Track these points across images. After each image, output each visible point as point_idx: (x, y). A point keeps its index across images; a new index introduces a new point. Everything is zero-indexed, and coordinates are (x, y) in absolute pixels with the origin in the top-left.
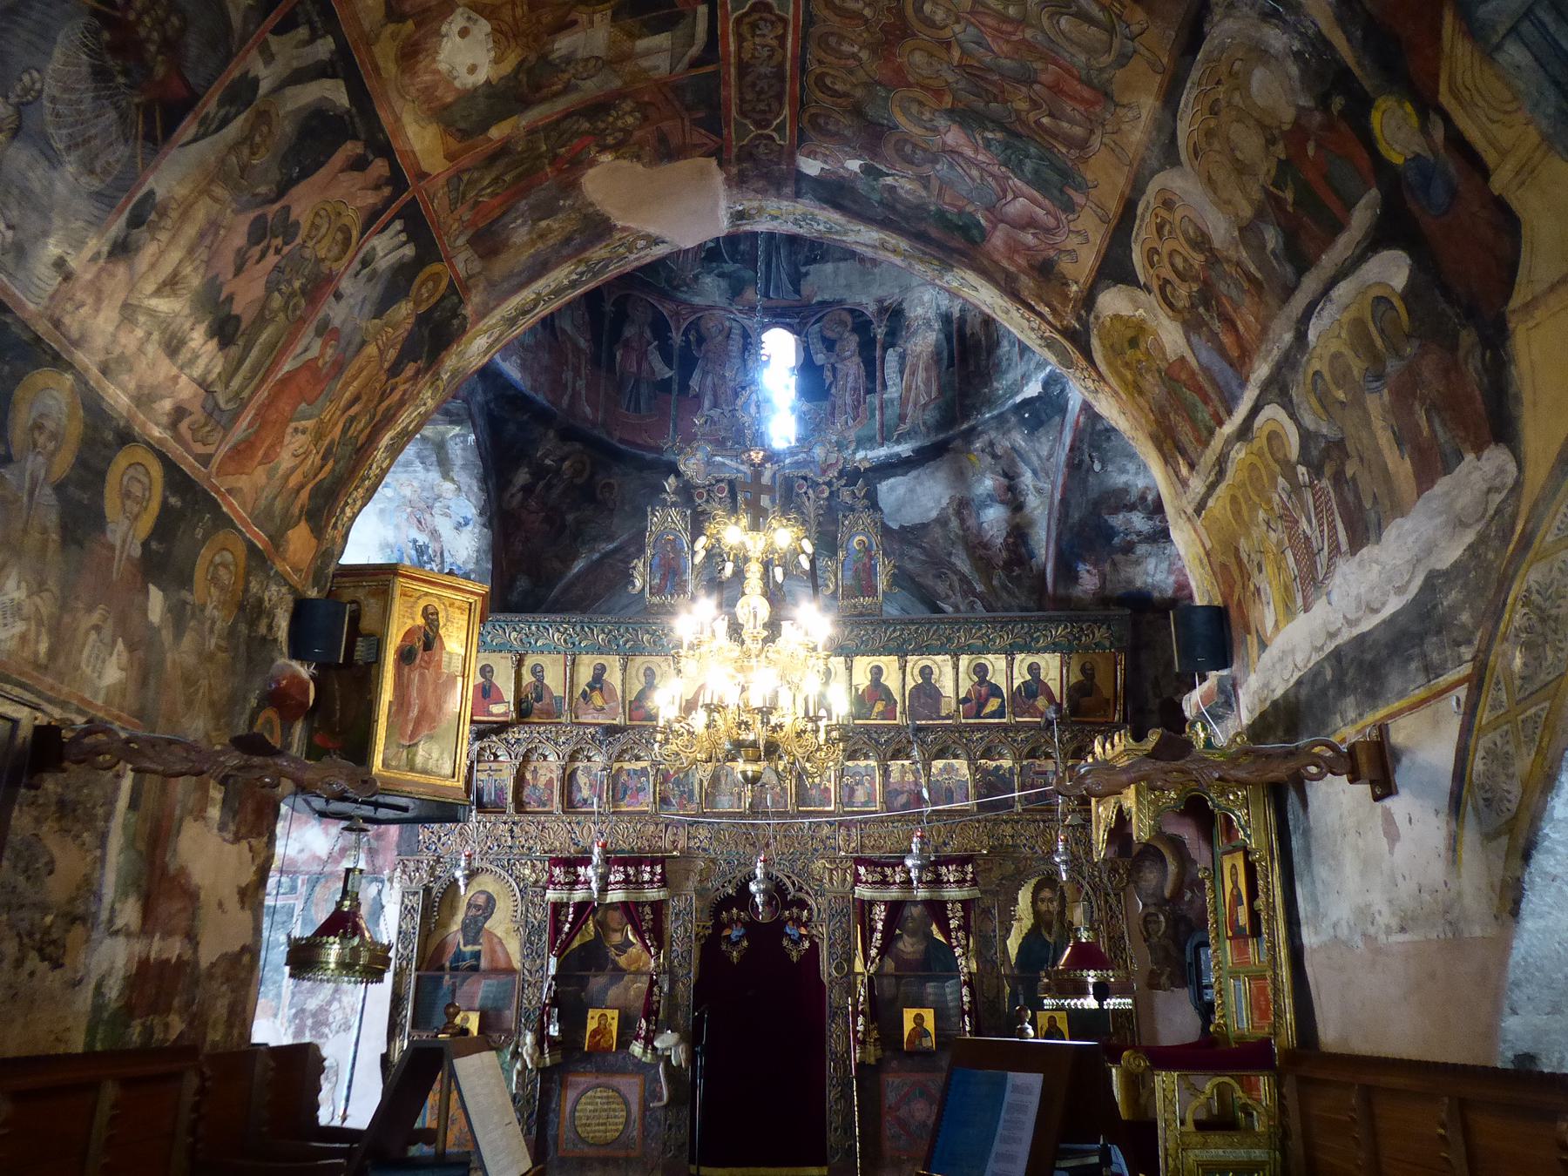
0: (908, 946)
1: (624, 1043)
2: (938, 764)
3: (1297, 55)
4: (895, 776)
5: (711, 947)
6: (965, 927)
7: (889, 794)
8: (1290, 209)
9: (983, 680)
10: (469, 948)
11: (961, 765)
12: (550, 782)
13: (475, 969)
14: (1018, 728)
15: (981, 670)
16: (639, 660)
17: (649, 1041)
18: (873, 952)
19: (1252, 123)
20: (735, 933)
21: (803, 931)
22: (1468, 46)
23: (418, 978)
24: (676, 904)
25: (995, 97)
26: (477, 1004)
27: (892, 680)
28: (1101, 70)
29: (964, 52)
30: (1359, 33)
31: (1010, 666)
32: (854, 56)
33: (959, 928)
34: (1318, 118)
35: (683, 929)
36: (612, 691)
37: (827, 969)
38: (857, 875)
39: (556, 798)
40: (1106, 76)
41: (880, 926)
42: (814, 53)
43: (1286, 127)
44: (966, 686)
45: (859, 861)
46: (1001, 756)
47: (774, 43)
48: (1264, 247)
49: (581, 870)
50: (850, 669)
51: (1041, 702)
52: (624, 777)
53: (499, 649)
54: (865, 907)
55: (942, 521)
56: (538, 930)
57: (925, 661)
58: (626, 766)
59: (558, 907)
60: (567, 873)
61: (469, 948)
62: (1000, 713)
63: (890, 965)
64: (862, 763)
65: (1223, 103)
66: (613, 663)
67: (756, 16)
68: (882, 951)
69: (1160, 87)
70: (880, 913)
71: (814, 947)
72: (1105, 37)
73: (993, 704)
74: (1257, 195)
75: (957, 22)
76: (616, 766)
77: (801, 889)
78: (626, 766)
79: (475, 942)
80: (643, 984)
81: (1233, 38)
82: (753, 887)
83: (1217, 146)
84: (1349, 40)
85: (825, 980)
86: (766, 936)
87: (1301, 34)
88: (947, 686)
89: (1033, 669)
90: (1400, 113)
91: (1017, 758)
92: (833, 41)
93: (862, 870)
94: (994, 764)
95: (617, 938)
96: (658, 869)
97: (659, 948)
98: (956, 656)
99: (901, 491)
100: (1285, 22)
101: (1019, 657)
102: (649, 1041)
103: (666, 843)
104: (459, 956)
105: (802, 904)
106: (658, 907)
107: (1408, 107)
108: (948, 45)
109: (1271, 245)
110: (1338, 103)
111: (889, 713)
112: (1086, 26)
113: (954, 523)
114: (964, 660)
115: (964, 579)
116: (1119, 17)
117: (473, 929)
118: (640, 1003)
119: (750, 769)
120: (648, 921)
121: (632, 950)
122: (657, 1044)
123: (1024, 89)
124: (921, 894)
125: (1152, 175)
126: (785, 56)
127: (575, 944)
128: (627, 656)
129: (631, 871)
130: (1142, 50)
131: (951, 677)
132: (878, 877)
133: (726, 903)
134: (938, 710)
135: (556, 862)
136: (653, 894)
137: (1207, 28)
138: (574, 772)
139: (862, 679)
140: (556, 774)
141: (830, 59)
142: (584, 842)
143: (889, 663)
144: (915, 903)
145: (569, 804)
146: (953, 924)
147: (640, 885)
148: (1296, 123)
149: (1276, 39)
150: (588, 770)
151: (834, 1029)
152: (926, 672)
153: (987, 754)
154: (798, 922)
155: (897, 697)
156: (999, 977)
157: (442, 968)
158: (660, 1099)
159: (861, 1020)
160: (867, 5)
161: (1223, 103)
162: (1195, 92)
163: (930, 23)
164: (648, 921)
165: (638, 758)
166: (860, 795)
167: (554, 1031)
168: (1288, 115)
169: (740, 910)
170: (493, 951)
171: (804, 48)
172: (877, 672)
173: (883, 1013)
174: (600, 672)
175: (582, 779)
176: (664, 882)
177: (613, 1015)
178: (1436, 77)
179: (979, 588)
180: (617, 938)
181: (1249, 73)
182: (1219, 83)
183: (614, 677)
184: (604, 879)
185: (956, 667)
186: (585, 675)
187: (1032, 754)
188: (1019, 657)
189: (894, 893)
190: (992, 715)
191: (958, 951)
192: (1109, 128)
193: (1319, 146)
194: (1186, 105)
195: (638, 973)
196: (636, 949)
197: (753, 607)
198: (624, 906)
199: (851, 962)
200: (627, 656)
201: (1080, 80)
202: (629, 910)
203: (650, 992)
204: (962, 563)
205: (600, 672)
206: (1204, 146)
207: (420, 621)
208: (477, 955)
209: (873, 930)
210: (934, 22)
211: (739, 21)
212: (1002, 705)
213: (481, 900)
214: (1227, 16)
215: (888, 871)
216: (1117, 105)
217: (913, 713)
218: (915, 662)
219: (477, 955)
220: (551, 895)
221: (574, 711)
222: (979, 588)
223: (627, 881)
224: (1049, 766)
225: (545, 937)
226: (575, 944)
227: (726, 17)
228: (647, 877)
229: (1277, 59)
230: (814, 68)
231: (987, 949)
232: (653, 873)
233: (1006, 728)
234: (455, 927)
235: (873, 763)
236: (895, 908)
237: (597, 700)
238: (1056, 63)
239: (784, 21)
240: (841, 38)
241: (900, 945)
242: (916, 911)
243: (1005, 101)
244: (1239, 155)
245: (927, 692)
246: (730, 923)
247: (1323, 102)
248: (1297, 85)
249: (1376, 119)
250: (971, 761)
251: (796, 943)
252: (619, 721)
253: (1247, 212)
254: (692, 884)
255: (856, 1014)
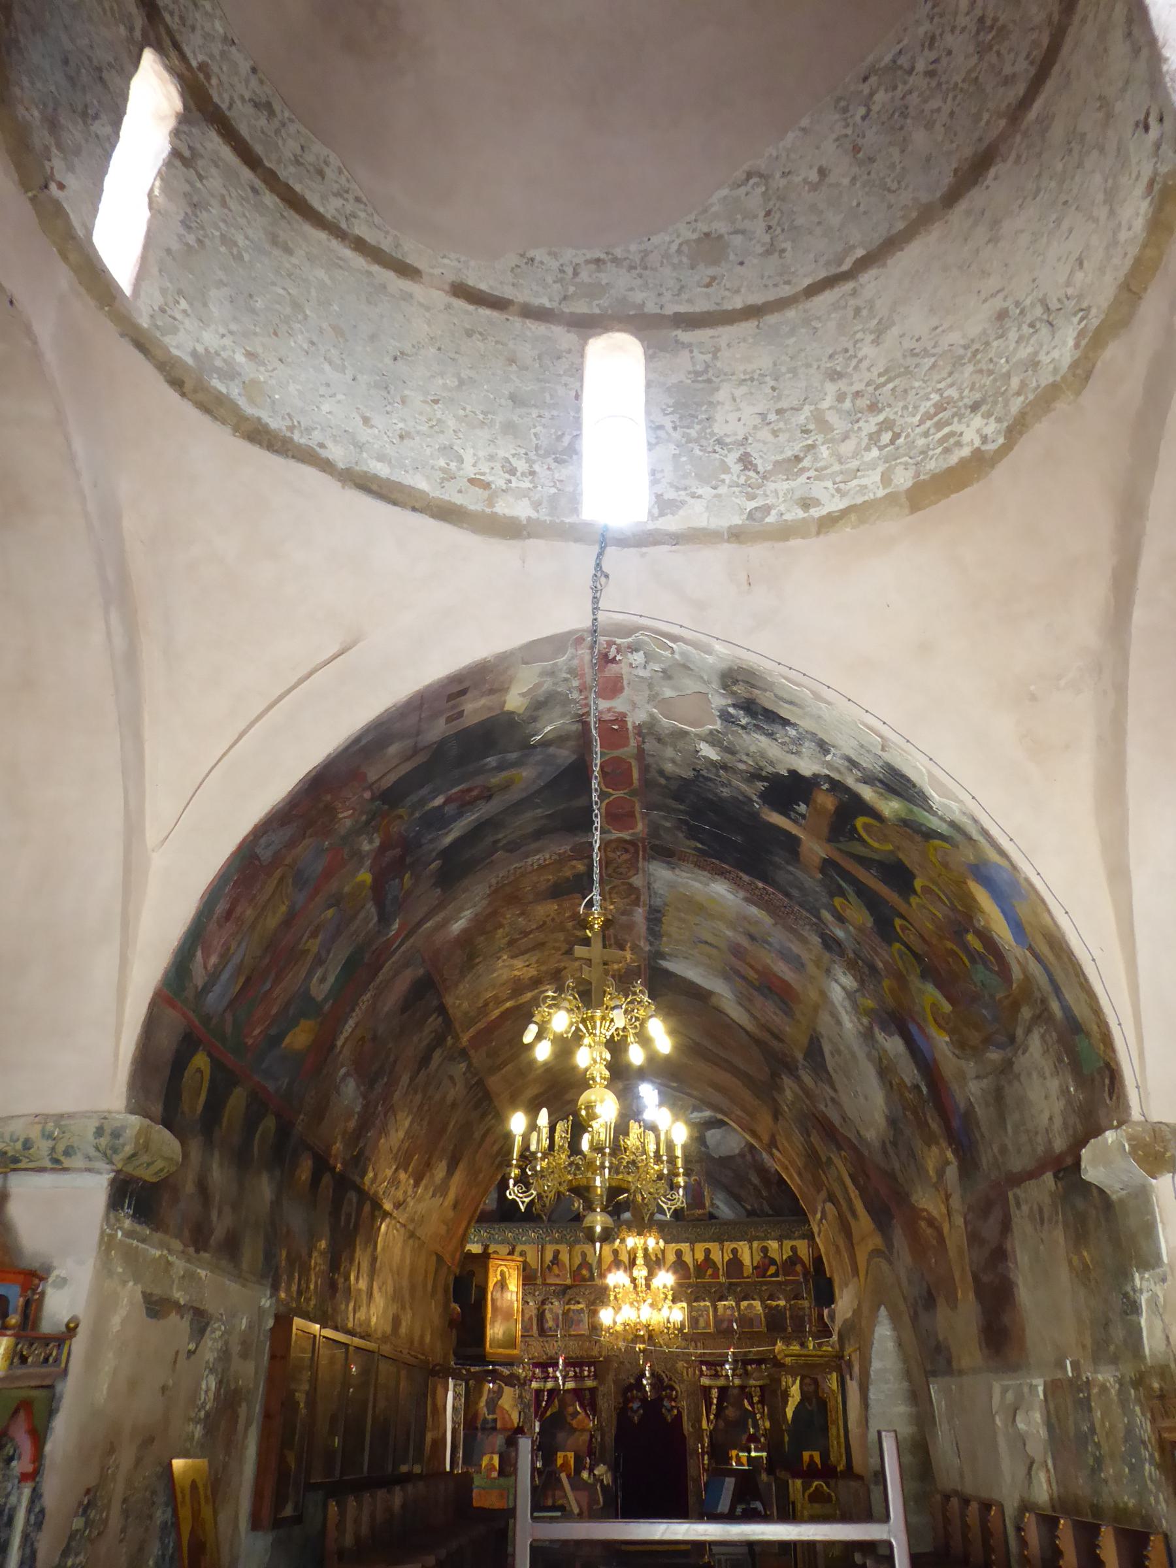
0: (731, 1412)
1: (578, 1471)
2: (744, 1304)
4: (720, 1311)
5: (623, 1413)
6: (762, 1402)
7: (718, 1321)
9: (766, 1255)
10: (491, 1417)
11: (757, 1304)
12: (531, 1318)
13: (494, 1429)
14: (786, 1283)
15: (765, 1250)
16: (578, 1247)
17: (591, 1471)
18: (712, 1417)
20: (635, 1405)
21: (673, 1404)
23: (465, 1435)
24: (602, 1389)
26: (497, 1449)
27: (716, 1256)
31: (781, 1246)
33: (759, 1402)
35: (607, 1404)
36: (564, 1264)
37: (687, 1426)
38: (701, 1371)
39: (535, 1327)
41: (715, 1401)
44: (757, 1259)
45: (702, 1363)
46: (779, 1299)
49: (550, 1370)
50: (693, 1250)
51: (799, 1268)
52: (571, 1314)
53: (502, 1242)
54: (707, 1390)
55: (742, 1155)
56: (528, 1406)
57: (734, 1245)
58: (572, 1307)
59: (538, 1392)
60: (542, 1372)
61: (491, 1417)
62: (776, 1274)
63: (721, 1424)
64: (702, 1304)
66: (563, 1248)
68: (716, 1416)
70: (715, 1393)
71: (680, 1414)
73: (772, 1270)
76: (567, 1307)
77: (670, 1379)
78: (572, 1307)
79: (494, 1413)
80: (586, 1437)
82: (645, 1382)
85: (686, 1433)
86: (653, 1407)
88: (746, 1259)
89: (793, 1249)
91: (787, 1301)
93: (704, 1368)
94: (774, 1303)
95: (571, 1409)
96: (592, 1369)
97: (594, 1416)
98: (750, 1241)
99: (719, 1137)
101: (785, 1242)
102: (591, 1471)
103: (595, 1353)
104: (485, 1420)
105: (672, 1388)
106: (593, 1391)
111: (715, 1275)
113: (749, 1157)
114: (755, 1244)
115: (755, 1187)
117: (493, 1405)
118: (585, 1449)
119: (642, 1346)
120: (586, 1398)
121: (579, 1417)
122: (596, 1472)
124: (737, 1382)
127: (548, 1413)
128: (571, 1246)
129: (577, 1370)
131: (747, 1254)
132: (713, 1372)
133: (630, 1387)
134: (742, 1273)
135: (536, 1365)
136: (590, 1383)
138: (544, 1311)
139: (700, 1256)
140: (534, 1312)
142: (551, 1352)
143: (714, 1247)
144: (734, 1387)
145: (542, 1331)
146: (756, 1399)
147: (582, 1378)
150: (551, 1310)
151: (691, 1463)
152: (735, 1251)
153: (771, 1298)
154: (671, 1399)
155: (720, 1266)
156: (782, 1431)
157: (476, 1428)
158: (598, 1503)
159: (706, 1457)
164: (586, 1398)
165: (579, 1303)
166: (702, 1323)
167: (539, 1465)
169: (638, 1391)
170: (504, 1418)
172: (708, 1252)
173: (719, 1453)
174: (557, 1254)
175: (548, 1316)
176: (596, 1377)
177: (571, 1455)
179: (765, 1194)
180: (571, 1409)
183: (564, 1257)
184: (565, 1377)
185: (751, 1248)
186: (549, 1256)
187: (796, 1298)
188: (785, 1242)
189: (721, 1382)
190: (771, 1276)
191: (758, 1416)
195: (583, 1430)
196: (582, 1415)
197: (640, 1272)
198: (574, 1390)
199: (700, 1422)
200: (571, 1246)
202: (576, 1392)
203: (591, 1441)
204: (755, 1180)
205: (557, 1254)
207: (499, 1278)
208: (495, 1420)
209: (711, 1404)
212: (777, 1270)
213: (496, 1388)
215: (719, 1368)
217: (728, 1275)
218: (729, 1246)
219: (495, 1420)
220: (534, 1385)
221: (544, 1278)
222: (765, 1194)
223: (575, 1376)
224: (806, 1303)
225: (532, 1410)
226: (548, 1413)
228: (586, 1373)
231: (776, 1415)
232: (589, 1371)
233: (779, 1283)
234: (483, 1403)
235: (708, 1304)
236: (723, 1390)
237: (556, 1270)
241: (727, 1412)
242: (736, 1391)
245: (735, 1264)
246: (632, 1400)
250: (762, 1302)
251: (670, 1410)
252: (569, 1282)
254: (610, 1377)
255: (703, 1454)
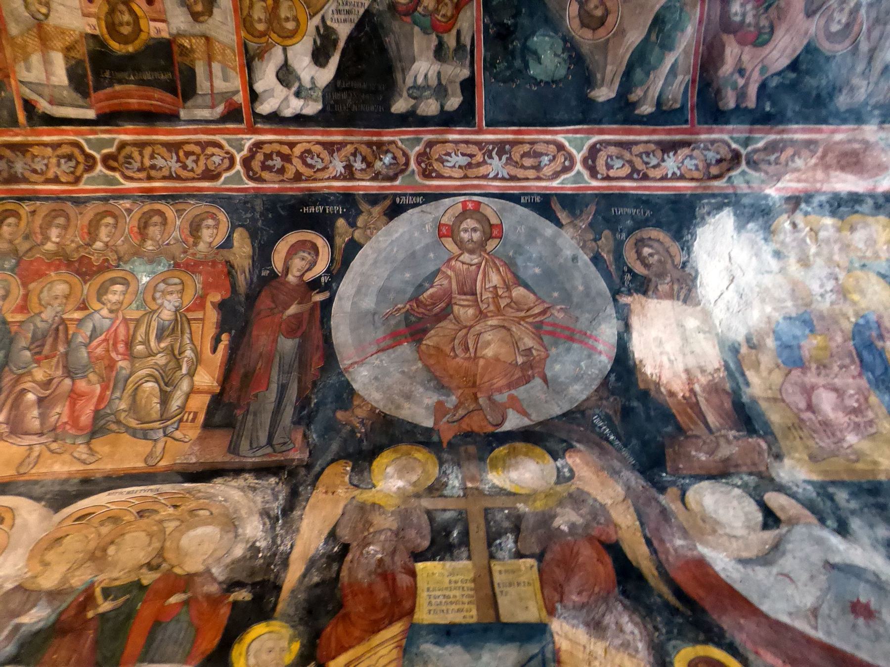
3: (254, 549)
8: (90, 614)
19: (157, 545)
22: (395, 654)
25: (39, 353)
28: (118, 422)
29: (80, 321)
30: (316, 579)
32: (47, 238)
34: (214, 588)
40: (114, 427)
42: (44, 208)
43: (178, 571)
47: (51, 175)
48: (18, 616)
65: (157, 517)
67: (81, 158)
69: (134, 468)
72: (155, 415)
74: (78, 581)
75: (111, 311)
81: (225, 501)
83: (104, 530)
84: (304, 576)
87: (274, 542)
90: (284, 643)
92: (61, 221)
100: (273, 528)
107: (296, 647)
108: (83, 306)
109: (25, 619)
110: (243, 595)
112: (156, 400)
116: (181, 420)
123: (60, 372)
125: (19, 494)
126: (36, 183)
130: (160, 445)
137: (219, 480)
141: (38, 220)
148: (190, 578)
149: (254, 529)
160: (107, 245)
161: (157, 517)
162: (150, 494)
163: (102, 291)
168: (193, 565)
171: (47, 199)
178: (342, 649)
181: (205, 523)
182: (175, 507)
192: (54, 446)
193: (186, 603)
194: (129, 493)
201: (96, 412)
206: (96, 521)
210: (106, 293)
211: (77, 145)
214: (242, 489)
216: (88, 443)
227: (77, 133)
229: (236, 536)
230: (26, 208)
238: (104, 389)
239: (77, 180)
240: (65, 228)
243: (38, 362)
244: (111, 550)
247: (233, 585)
248: (228, 560)
249: (259, 629)
253: (49, 581)
